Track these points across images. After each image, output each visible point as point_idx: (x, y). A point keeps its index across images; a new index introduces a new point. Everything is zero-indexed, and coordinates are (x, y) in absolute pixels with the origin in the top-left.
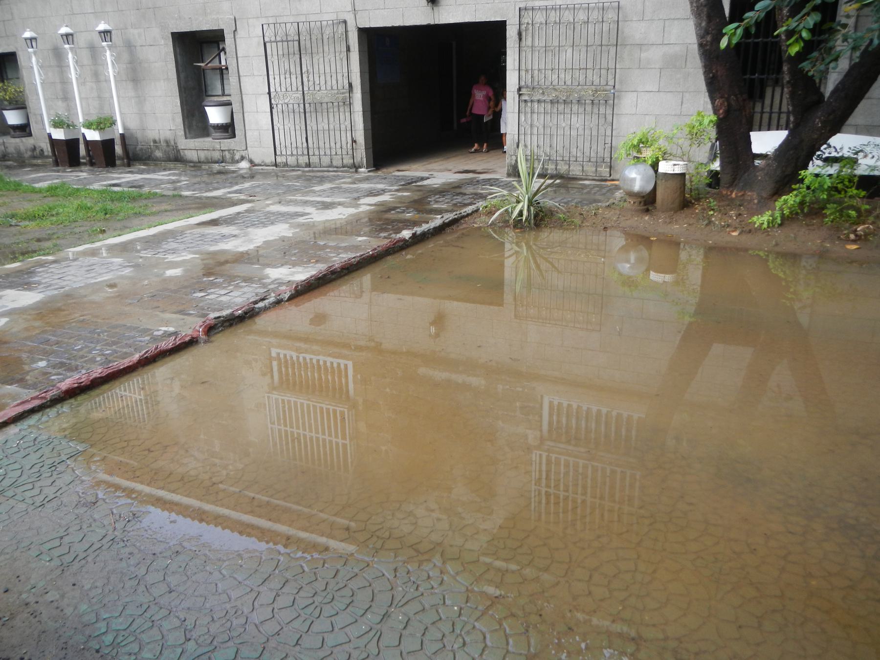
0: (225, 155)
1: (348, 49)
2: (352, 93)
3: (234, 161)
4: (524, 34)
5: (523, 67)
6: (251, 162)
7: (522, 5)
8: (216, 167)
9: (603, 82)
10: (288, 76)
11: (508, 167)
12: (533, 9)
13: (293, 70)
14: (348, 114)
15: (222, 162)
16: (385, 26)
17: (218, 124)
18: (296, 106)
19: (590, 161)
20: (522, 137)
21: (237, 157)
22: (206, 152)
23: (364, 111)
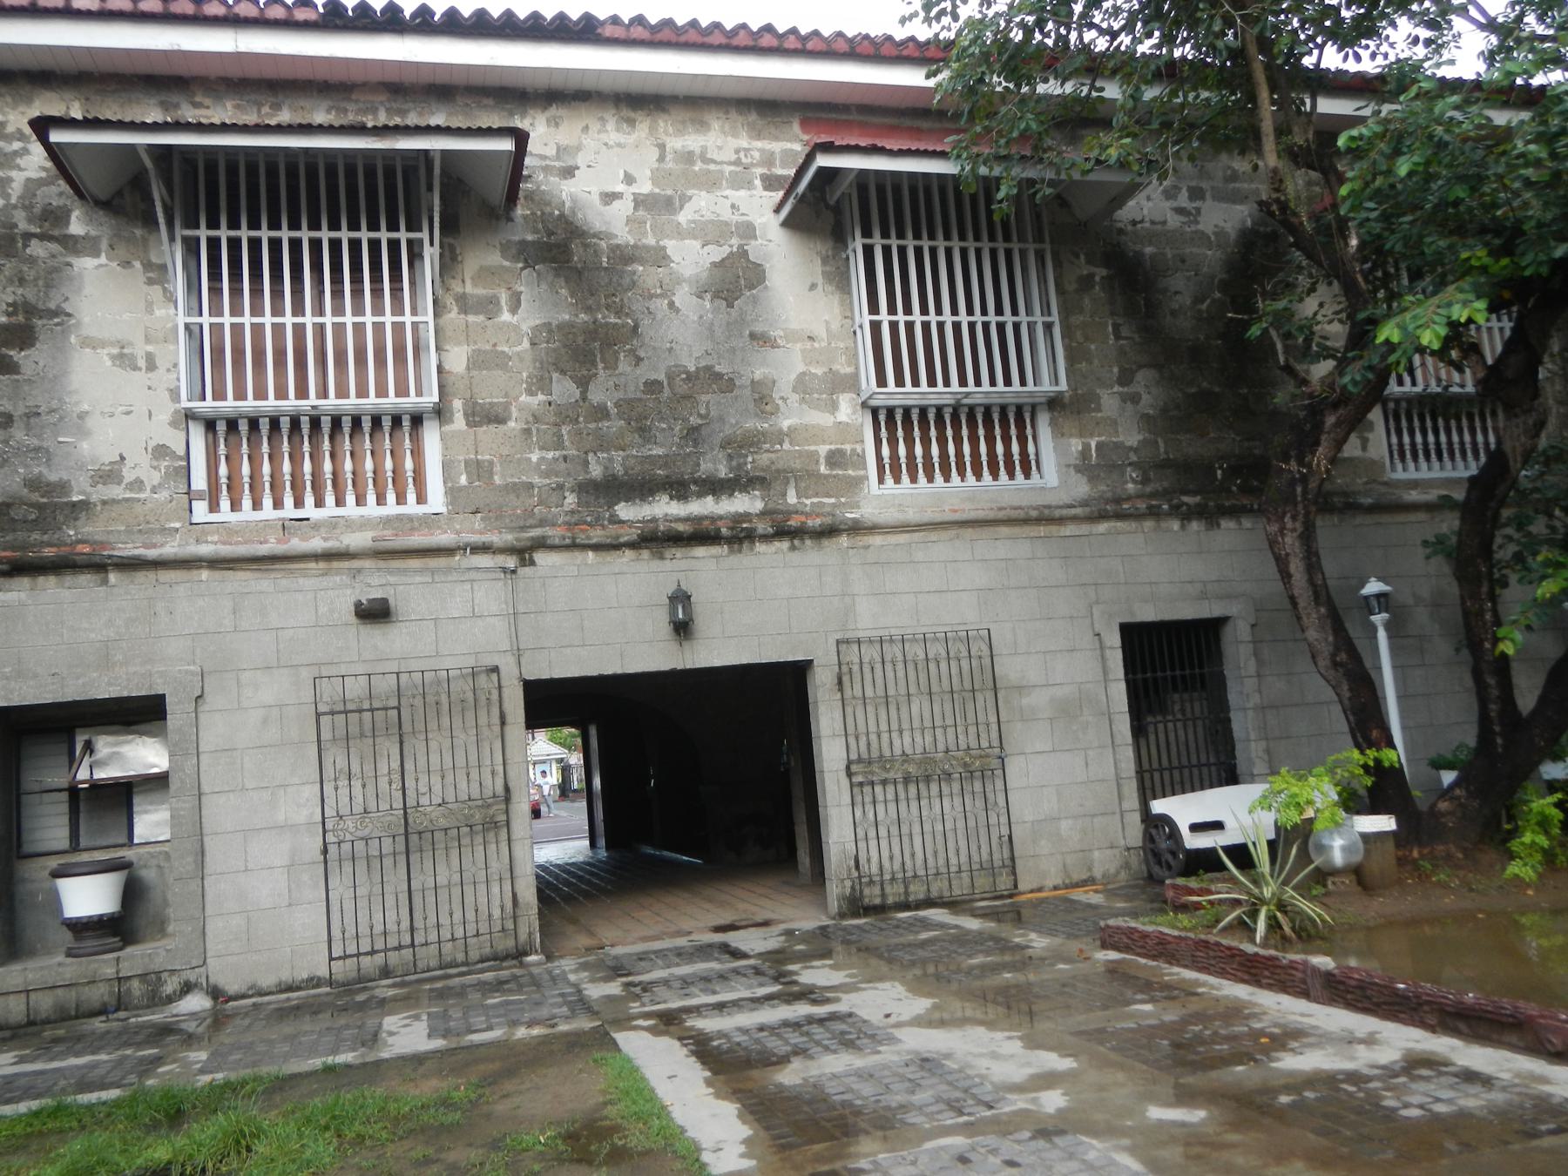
0: (129, 990)
1: (503, 723)
3: (156, 1000)
4: (846, 679)
5: (851, 729)
6: (215, 993)
7: (839, 636)
8: (98, 1024)
9: (985, 744)
10: (343, 783)
11: (839, 901)
12: (859, 642)
13: (355, 768)
15: (117, 1009)
16: (583, 674)
17: (101, 916)
18: (387, 843)
19: (982, 868)
20: (862, 845)
21: (170, 986)
22: (60, 992)
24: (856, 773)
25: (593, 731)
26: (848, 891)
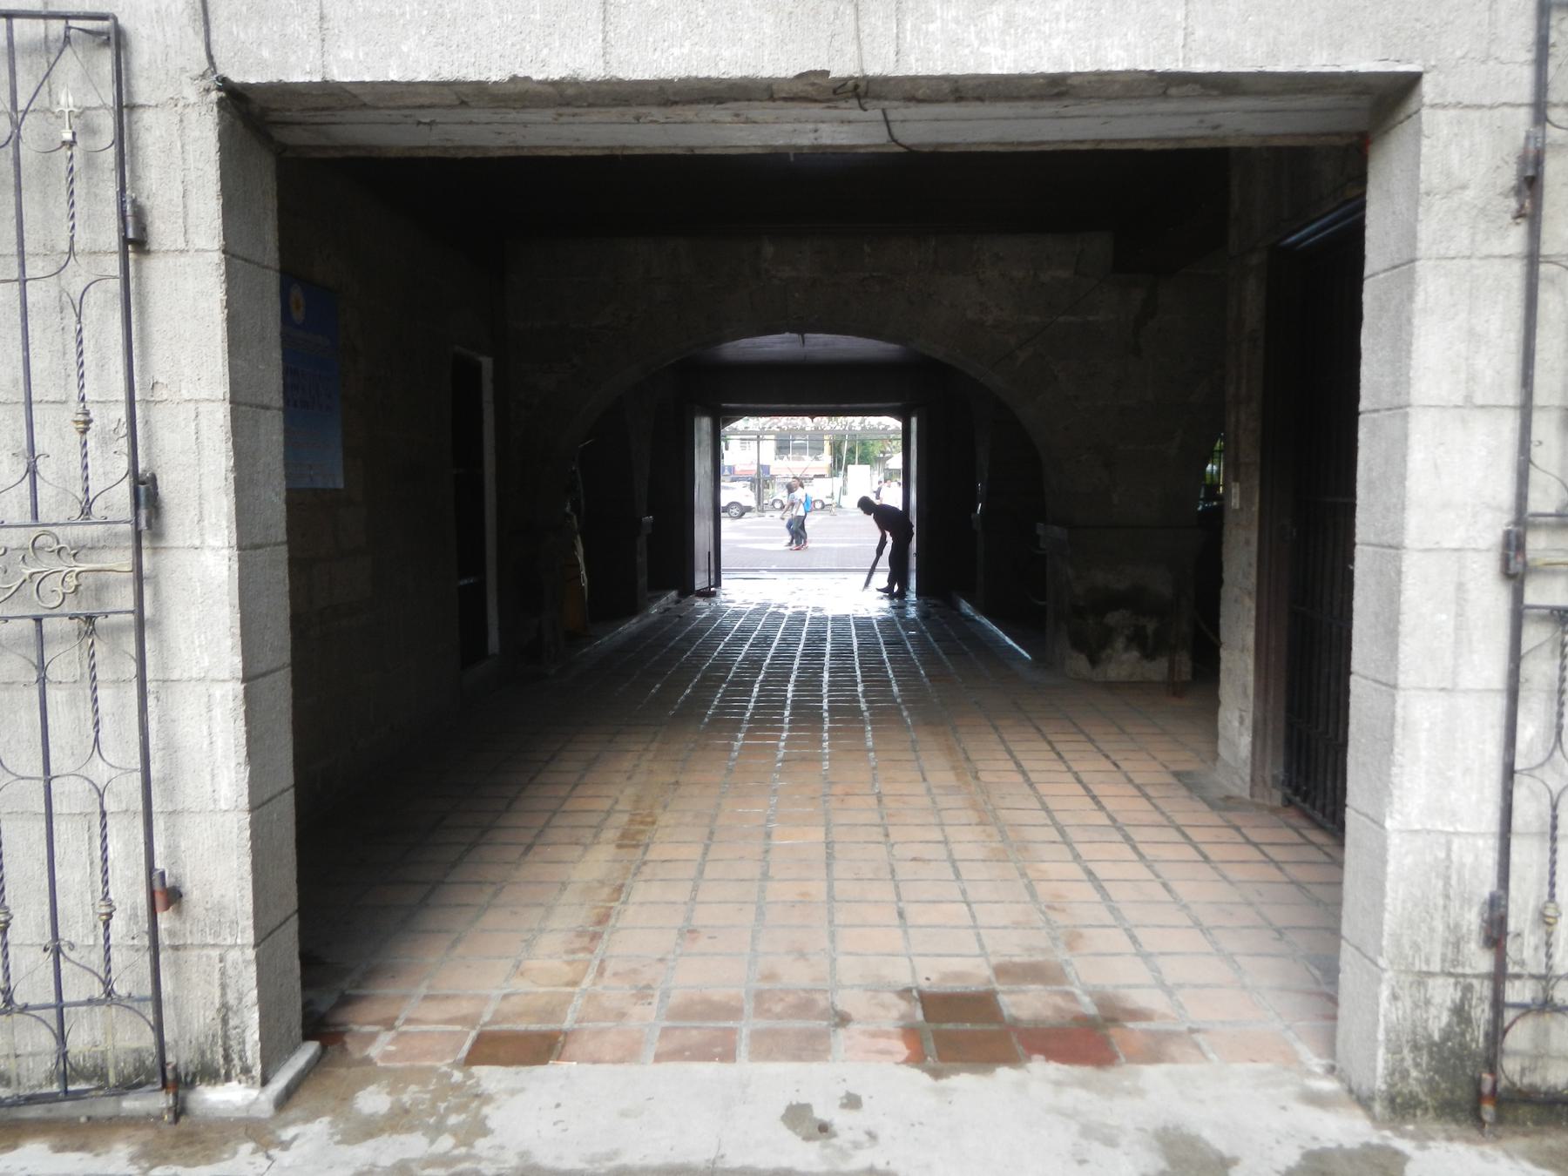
2: (155, 550)
11: (1394, 1049)
14: (117, 702)
16: (448, 73)
23: (250, 678)
24: (1550, 570)
25: (914, 421)
26: (1438, 1021)
